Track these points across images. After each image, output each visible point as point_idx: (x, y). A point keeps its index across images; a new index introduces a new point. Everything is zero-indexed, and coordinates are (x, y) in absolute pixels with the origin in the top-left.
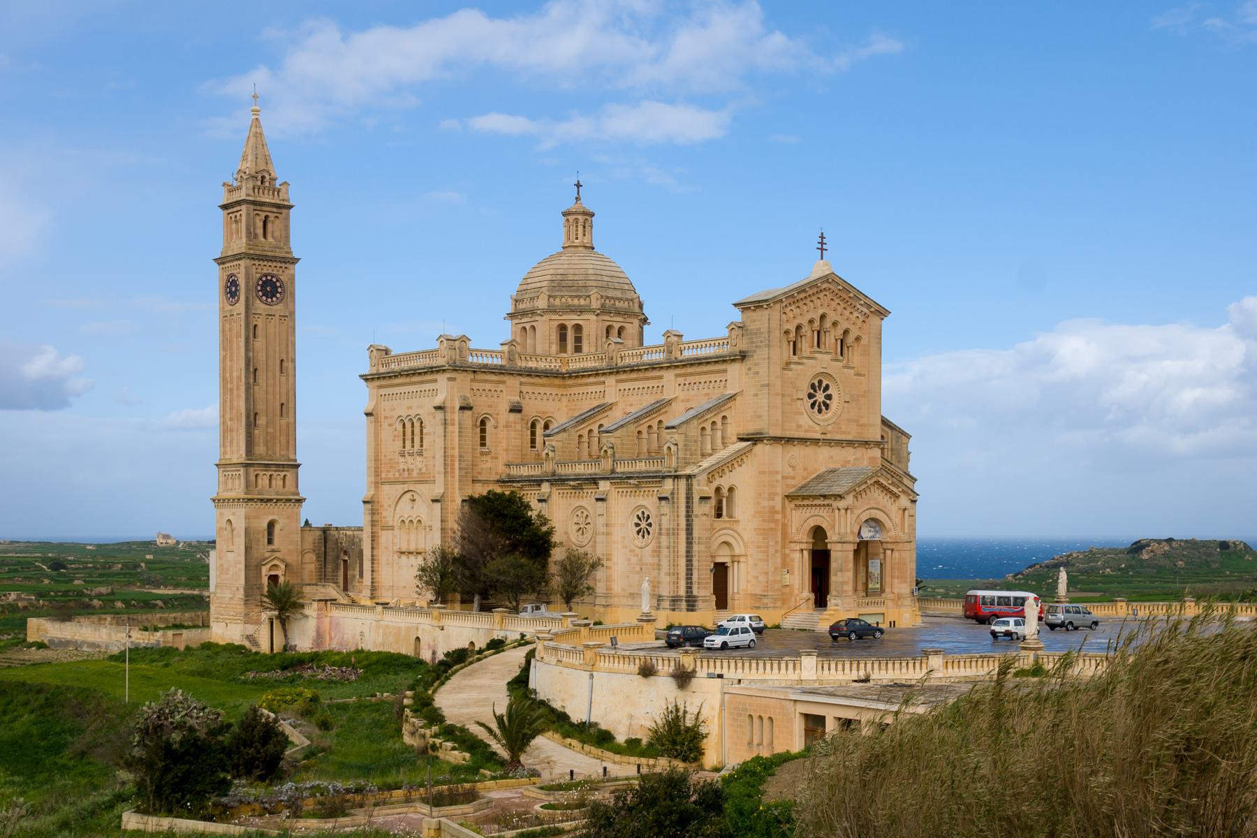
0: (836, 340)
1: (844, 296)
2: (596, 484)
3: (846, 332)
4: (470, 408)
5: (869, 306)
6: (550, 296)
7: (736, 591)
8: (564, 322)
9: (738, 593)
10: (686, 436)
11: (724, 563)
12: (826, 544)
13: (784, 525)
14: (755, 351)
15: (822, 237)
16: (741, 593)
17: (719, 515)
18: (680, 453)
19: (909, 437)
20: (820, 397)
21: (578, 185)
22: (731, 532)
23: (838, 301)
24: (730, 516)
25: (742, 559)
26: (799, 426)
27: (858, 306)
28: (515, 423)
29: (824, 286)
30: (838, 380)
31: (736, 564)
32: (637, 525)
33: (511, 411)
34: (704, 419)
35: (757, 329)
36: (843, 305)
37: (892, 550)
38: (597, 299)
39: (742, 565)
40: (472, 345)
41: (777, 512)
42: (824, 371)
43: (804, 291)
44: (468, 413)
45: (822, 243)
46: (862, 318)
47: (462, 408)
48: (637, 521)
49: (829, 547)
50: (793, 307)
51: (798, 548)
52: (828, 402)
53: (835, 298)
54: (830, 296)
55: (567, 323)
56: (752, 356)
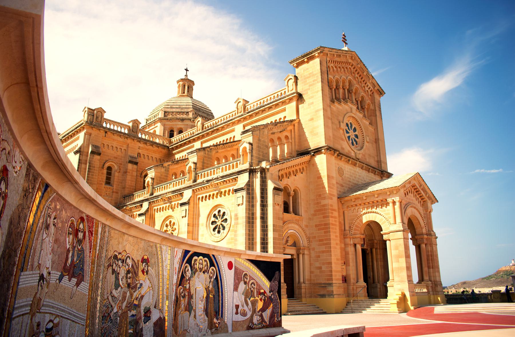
0: (357, 101)
2: (181, 195)
3: (363, 97)
4: (99, 154)
6: (165, 112)
7: (302, 280)
8: (172, 126)
9: (304, 283)
10: (259, 140)
12: (382, 235)
13: (340, 223)
14: (309, 89)
16: (307, 282)
17: (286, 210)
18: (254, 152)
20: (352, 134)
21: (187, 70)
22: (297, 227)
23: (357, 76)
24: (296, 212)
25: (306, 252)
26: (343, 149)
28: (133, 171)
29: (350, 61)
31: (301, 256)
32: (213, 223)
33: (130, 162)
34: (272, 132)
35: (310, 74)
37: (426, 245)
38: (193, 114)
39: (306, 257)
40: (106, 116)
41: (334, 210)
42: (353, 115)
44: (97, 157)
45: (344, 39)
47: (92, 152)
48: (213, 219)
49: (385, 237)
51: (352, 242)
52: (357, 139)
55: (174, 127)
56: (307, 93)
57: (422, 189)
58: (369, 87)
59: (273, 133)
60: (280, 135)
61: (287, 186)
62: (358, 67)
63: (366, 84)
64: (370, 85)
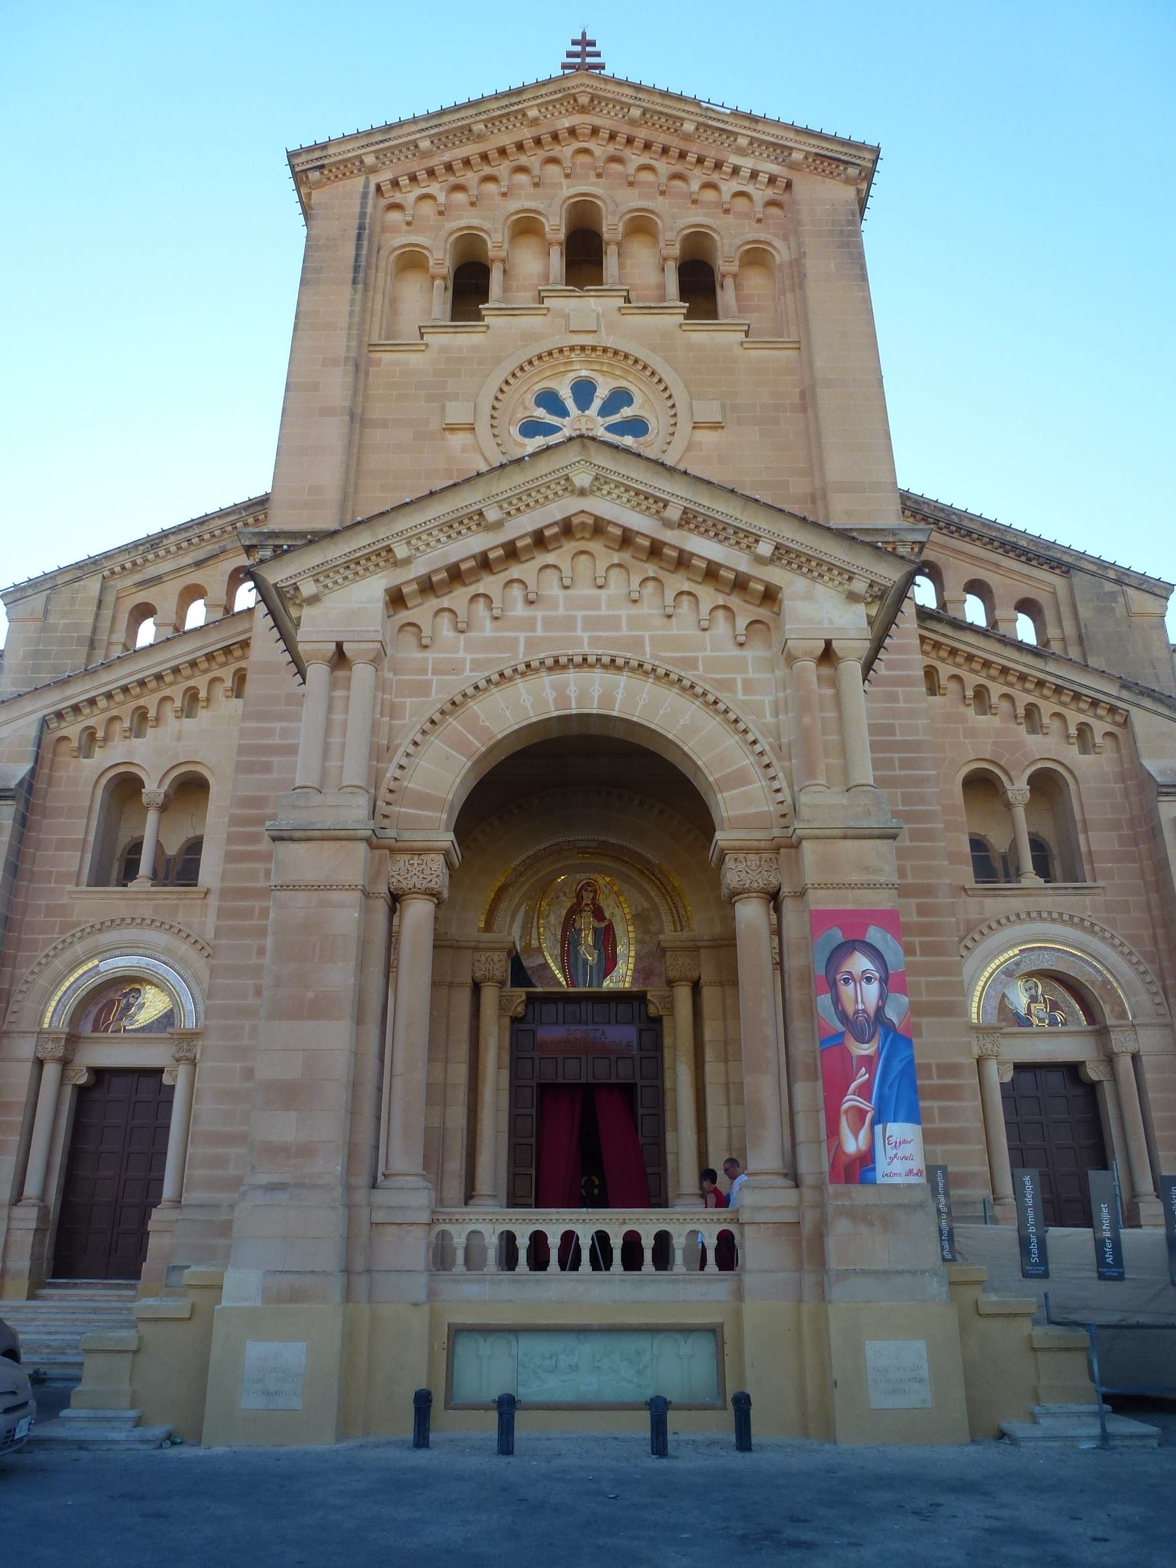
1: (662, 138)
5: (780, 150)
10: (46, 628)
11: (160, 1071)
15: (585, 42)
19: (1158, 590)
22: (161, 938)
23: (645, 159)
27: (734, 160)
29: (566, 123)
30: (656, 362)
34: (138, 577)
36: (664, 167)
37: (774, 898)
43: (466, 133)
46: (760, 193)
50: (434, 188)
53: (627, 153)
54: (600, 149)
57: (689, 520)
58: (745, 173)
59: (158, 580)
60: (197, 577)
61: (133, 770)
62: (633, 122)
63: (718, 166)
64: (747, 164)
